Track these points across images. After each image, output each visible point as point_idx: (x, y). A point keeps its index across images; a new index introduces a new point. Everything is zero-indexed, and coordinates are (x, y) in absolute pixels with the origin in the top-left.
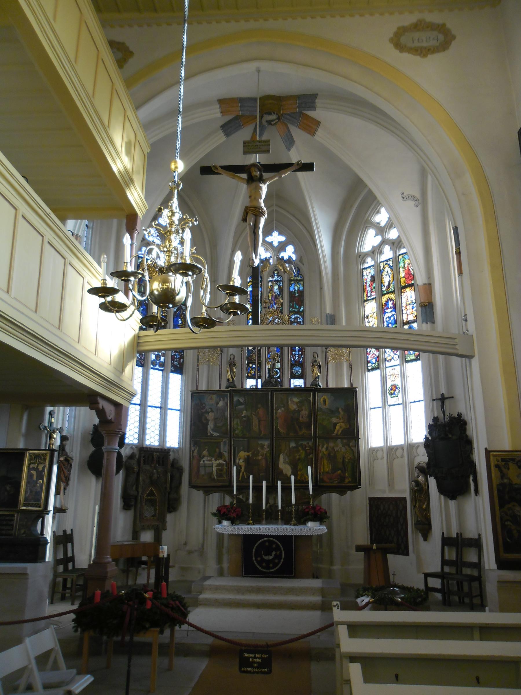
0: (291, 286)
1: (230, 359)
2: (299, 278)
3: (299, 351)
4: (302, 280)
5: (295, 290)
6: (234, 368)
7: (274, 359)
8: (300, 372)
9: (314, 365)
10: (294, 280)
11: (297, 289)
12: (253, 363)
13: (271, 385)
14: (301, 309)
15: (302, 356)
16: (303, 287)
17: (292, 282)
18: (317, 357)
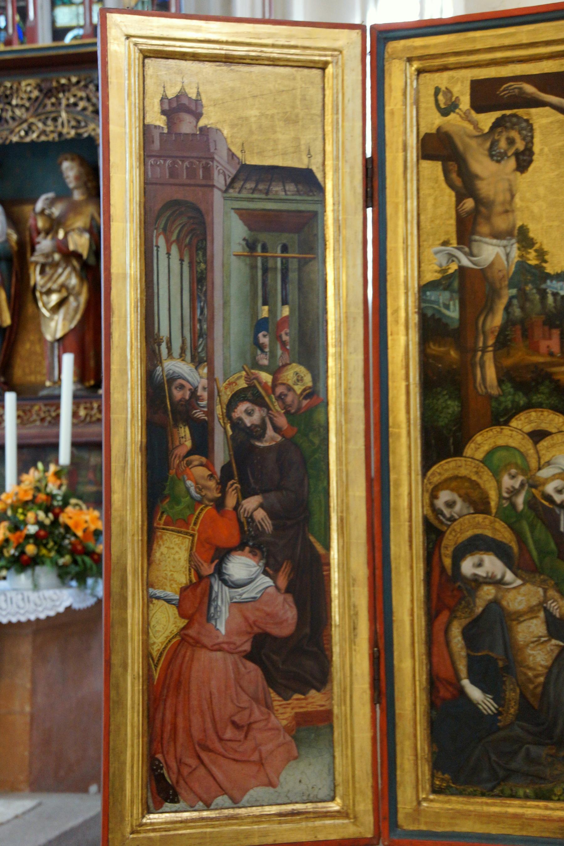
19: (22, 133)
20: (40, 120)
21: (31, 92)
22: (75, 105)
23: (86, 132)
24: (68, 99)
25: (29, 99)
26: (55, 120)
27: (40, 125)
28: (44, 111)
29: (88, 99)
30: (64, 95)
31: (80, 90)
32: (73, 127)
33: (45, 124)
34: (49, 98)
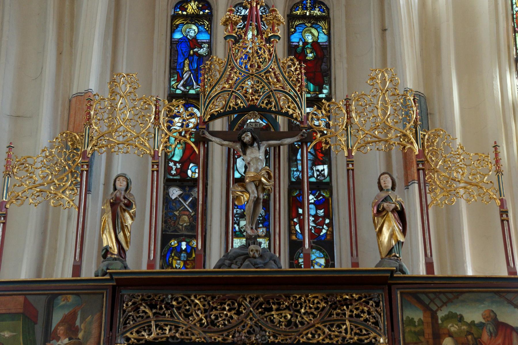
0: (293, 33)
1: (115, 189)
2: (317, 12)
3: (318, 205)
4: (326, 19)
5: (305, 43)
6: (127, 215)
7: (257, 187)
8: (320, 265)
9: (384, 209)
10: (303, 17)
11: (310, 41)
12: (182, 235)
13: (247, 262)
14: (321, 93)
15: (327, 221)
16: (329, 35)
17: (297, 23)
18: (393, 188)
19: (310, 336)
20: (325, 326)
21: (318, 303)
22: (358, 316)
23: (367, 339)
24: (351, 311)
25: (317, 308)
26: (339, 327)
27: (326, 330)
28: (329, 319)
29: (369, 313)
30: (348, 308)
31: (361, 304)
32: (356, 334)
33: (330, 330)
34: (335, 309)
